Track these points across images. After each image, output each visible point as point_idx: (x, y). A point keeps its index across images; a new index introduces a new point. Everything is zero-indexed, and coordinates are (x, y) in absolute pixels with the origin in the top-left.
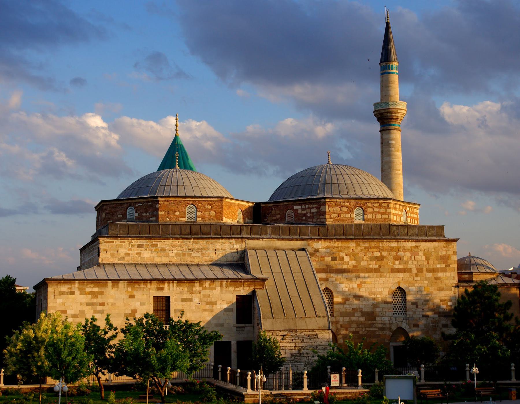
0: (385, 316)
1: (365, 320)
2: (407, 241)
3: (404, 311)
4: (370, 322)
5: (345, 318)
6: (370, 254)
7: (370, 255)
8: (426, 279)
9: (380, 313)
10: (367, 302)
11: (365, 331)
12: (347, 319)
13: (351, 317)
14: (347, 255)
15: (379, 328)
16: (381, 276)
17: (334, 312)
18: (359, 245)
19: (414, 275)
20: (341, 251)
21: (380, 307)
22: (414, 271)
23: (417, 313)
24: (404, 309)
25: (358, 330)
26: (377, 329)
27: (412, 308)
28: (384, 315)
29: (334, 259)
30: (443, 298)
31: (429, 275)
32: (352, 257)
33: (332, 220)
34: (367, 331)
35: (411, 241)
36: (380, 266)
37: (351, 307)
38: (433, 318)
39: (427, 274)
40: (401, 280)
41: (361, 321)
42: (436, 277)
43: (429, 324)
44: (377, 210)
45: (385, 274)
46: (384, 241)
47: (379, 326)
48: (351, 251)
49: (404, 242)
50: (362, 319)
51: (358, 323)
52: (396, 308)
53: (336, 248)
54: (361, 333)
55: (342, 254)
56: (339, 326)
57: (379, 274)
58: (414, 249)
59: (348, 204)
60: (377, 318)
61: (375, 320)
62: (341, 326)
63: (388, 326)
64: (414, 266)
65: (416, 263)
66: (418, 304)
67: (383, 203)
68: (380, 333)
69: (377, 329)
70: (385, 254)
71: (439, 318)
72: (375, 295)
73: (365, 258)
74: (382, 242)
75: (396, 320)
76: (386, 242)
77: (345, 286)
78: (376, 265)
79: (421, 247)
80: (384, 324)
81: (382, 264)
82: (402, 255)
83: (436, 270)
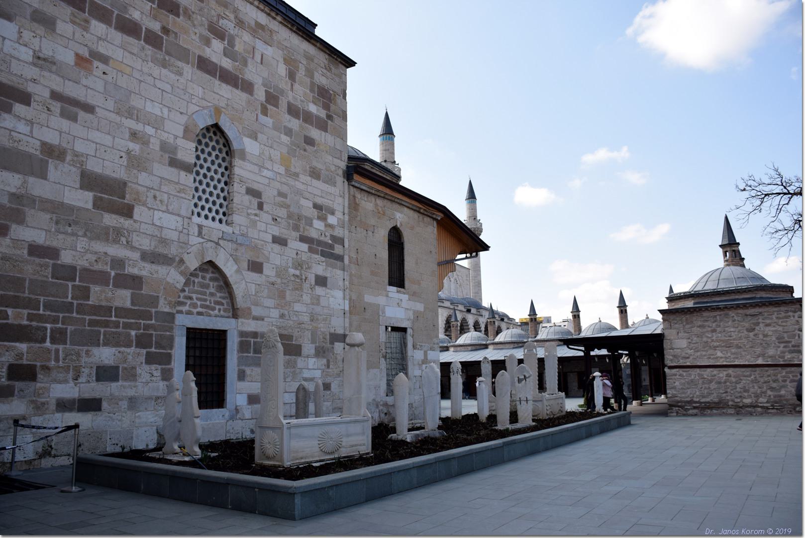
0: (167, 211)
9: (150, 194)
11: (87, 251)
13: (31, 180)
21: (151, 174)
22: (260, 94)
28: (164, 208)
30: (319, 201)
31: (295, 124)
34: (96, 253)
47: (146, 244)
54: (66, 258)
57: (160, 55)
75: (200, 234)
80: (163, 241)
83: (308, 118)
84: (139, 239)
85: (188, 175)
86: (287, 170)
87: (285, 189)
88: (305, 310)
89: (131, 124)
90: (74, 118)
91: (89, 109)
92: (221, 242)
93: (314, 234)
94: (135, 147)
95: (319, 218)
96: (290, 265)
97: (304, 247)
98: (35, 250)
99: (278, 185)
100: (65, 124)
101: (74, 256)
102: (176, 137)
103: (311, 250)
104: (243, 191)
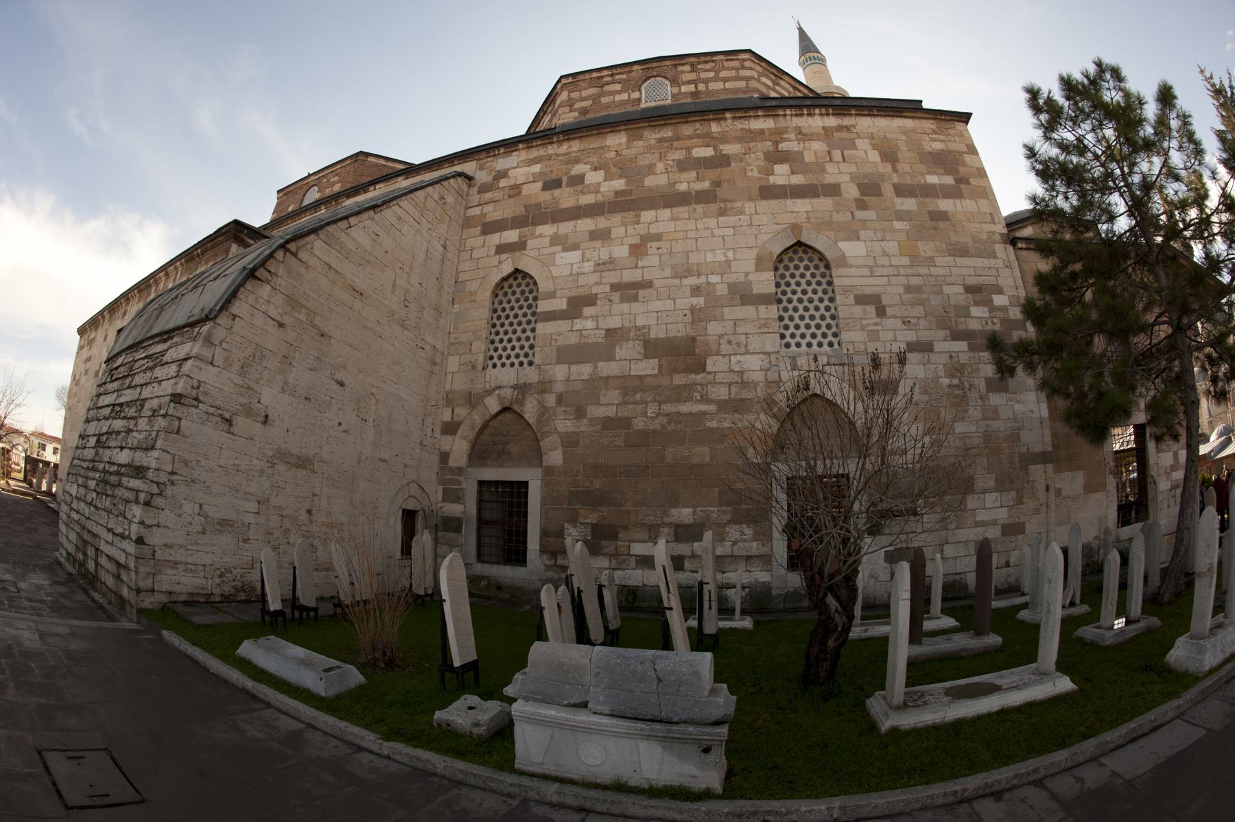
0: (747, 353)
1: (656, 372)
2: (805, 112)
3: (829, 333)
4: (679, 380)
5: (574, 368)
6: (679, 155)
7: (677, 158)
8: (901, 216)
10: (669, 302)
11: (658, 415)
12: (583, 371)
13: (600, 364)
14: (595, 169)
15: (718, 402)
16: (723, 212)
17: (537, 349)
18: (640, 138)
19: (853, 205)
20: (577, 161)
21: (723, 320)
22: (851, 191)
23: (886, 336)
24: (829, 327)
25: (626, 412)
26: (712, 408)
27: (861, 319)
29: (552, 184)
31: (909, 204)
32: (614, 170)
33: (576, 114)
34: (668, 415)
35: (821, 115)
36: (717, 183)
37: (601, 326)
38: (951, 357)
39: (898, 201)
40: (801, 219)
41: (640, 377)
42: (933, 211)
43: (936, 379)
44: (712, 74)
45: (739, 204)
46: (725, 119)
47: (721, 393)
48: (613, 154)
49: (796, 115)
50: (648, 367)
51: (630, 386)
52: (797, 321)
53: (562, 158)
54: (639, 424)
55: (578, 169)
56: (551, 400)
57: (713, 207)
58: (836, 134)
59: (624, 76)
60: (709, 361)
61: (701, 368)
62: (560, 400)
63: (760, 392)
64: (847, 178)
65: (852, 168)
66: (884, 302)
67: (727, 60)
68: (726, 425)
69: (712, 408)
70: (730, 149)
71: (971, 354)
72: (699, 275)
73: (660, 167)
74: (718, 120)
76: (735, 118)
77: (583, 256)
78: (704, 181)
79: (858, 129)
80: (744, 384)
81: (724, 177)
82: (796, 149)
84: (714, 390)
85: (769, 307)
86: (912, 257)
87: (915, 281)
88: (974, 429)
89: (693, 281)
90: (635, 299)
91: (648, 284)
92: (827, 369)
93: (974, 325)
94: (699, 301)
95: (977, 304)
96: (942, 373)
97: (962, 346)
98: (608, 423)
99: (903, 280)
100: (625, 307)
101: (645, 422)
102: (747, 274)
103: (972, 348)
104: (851, 300)
